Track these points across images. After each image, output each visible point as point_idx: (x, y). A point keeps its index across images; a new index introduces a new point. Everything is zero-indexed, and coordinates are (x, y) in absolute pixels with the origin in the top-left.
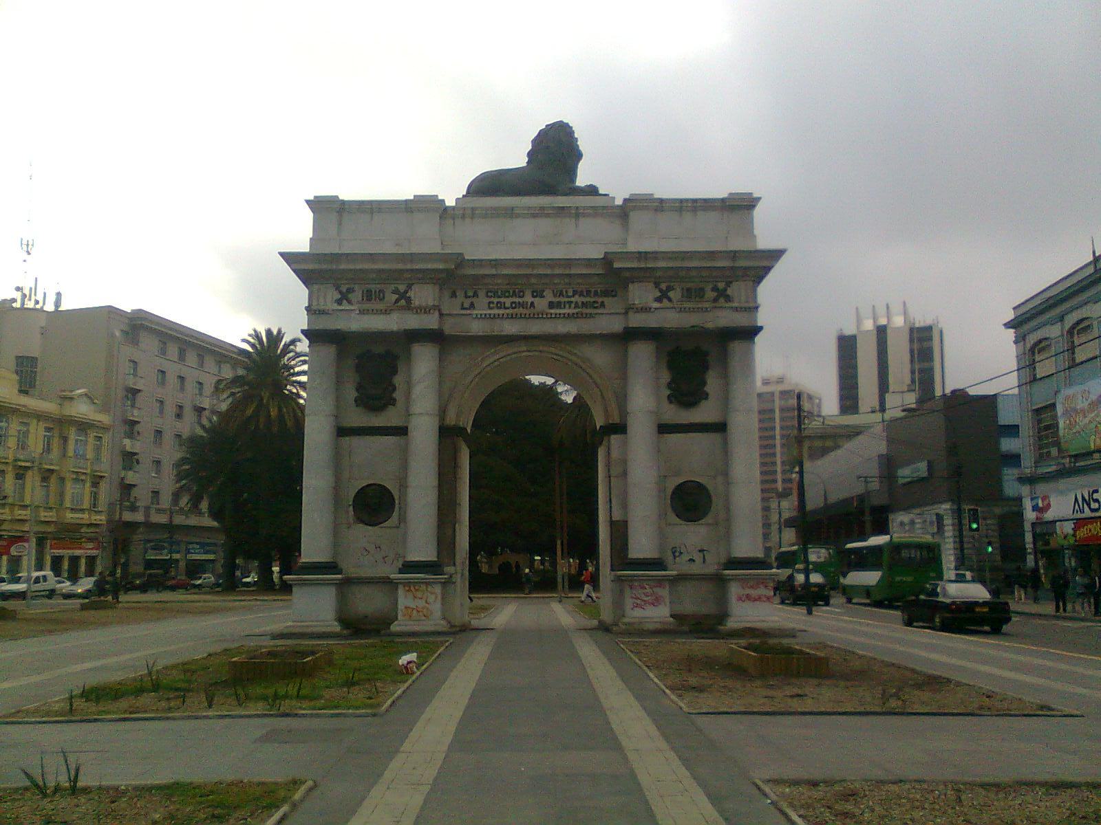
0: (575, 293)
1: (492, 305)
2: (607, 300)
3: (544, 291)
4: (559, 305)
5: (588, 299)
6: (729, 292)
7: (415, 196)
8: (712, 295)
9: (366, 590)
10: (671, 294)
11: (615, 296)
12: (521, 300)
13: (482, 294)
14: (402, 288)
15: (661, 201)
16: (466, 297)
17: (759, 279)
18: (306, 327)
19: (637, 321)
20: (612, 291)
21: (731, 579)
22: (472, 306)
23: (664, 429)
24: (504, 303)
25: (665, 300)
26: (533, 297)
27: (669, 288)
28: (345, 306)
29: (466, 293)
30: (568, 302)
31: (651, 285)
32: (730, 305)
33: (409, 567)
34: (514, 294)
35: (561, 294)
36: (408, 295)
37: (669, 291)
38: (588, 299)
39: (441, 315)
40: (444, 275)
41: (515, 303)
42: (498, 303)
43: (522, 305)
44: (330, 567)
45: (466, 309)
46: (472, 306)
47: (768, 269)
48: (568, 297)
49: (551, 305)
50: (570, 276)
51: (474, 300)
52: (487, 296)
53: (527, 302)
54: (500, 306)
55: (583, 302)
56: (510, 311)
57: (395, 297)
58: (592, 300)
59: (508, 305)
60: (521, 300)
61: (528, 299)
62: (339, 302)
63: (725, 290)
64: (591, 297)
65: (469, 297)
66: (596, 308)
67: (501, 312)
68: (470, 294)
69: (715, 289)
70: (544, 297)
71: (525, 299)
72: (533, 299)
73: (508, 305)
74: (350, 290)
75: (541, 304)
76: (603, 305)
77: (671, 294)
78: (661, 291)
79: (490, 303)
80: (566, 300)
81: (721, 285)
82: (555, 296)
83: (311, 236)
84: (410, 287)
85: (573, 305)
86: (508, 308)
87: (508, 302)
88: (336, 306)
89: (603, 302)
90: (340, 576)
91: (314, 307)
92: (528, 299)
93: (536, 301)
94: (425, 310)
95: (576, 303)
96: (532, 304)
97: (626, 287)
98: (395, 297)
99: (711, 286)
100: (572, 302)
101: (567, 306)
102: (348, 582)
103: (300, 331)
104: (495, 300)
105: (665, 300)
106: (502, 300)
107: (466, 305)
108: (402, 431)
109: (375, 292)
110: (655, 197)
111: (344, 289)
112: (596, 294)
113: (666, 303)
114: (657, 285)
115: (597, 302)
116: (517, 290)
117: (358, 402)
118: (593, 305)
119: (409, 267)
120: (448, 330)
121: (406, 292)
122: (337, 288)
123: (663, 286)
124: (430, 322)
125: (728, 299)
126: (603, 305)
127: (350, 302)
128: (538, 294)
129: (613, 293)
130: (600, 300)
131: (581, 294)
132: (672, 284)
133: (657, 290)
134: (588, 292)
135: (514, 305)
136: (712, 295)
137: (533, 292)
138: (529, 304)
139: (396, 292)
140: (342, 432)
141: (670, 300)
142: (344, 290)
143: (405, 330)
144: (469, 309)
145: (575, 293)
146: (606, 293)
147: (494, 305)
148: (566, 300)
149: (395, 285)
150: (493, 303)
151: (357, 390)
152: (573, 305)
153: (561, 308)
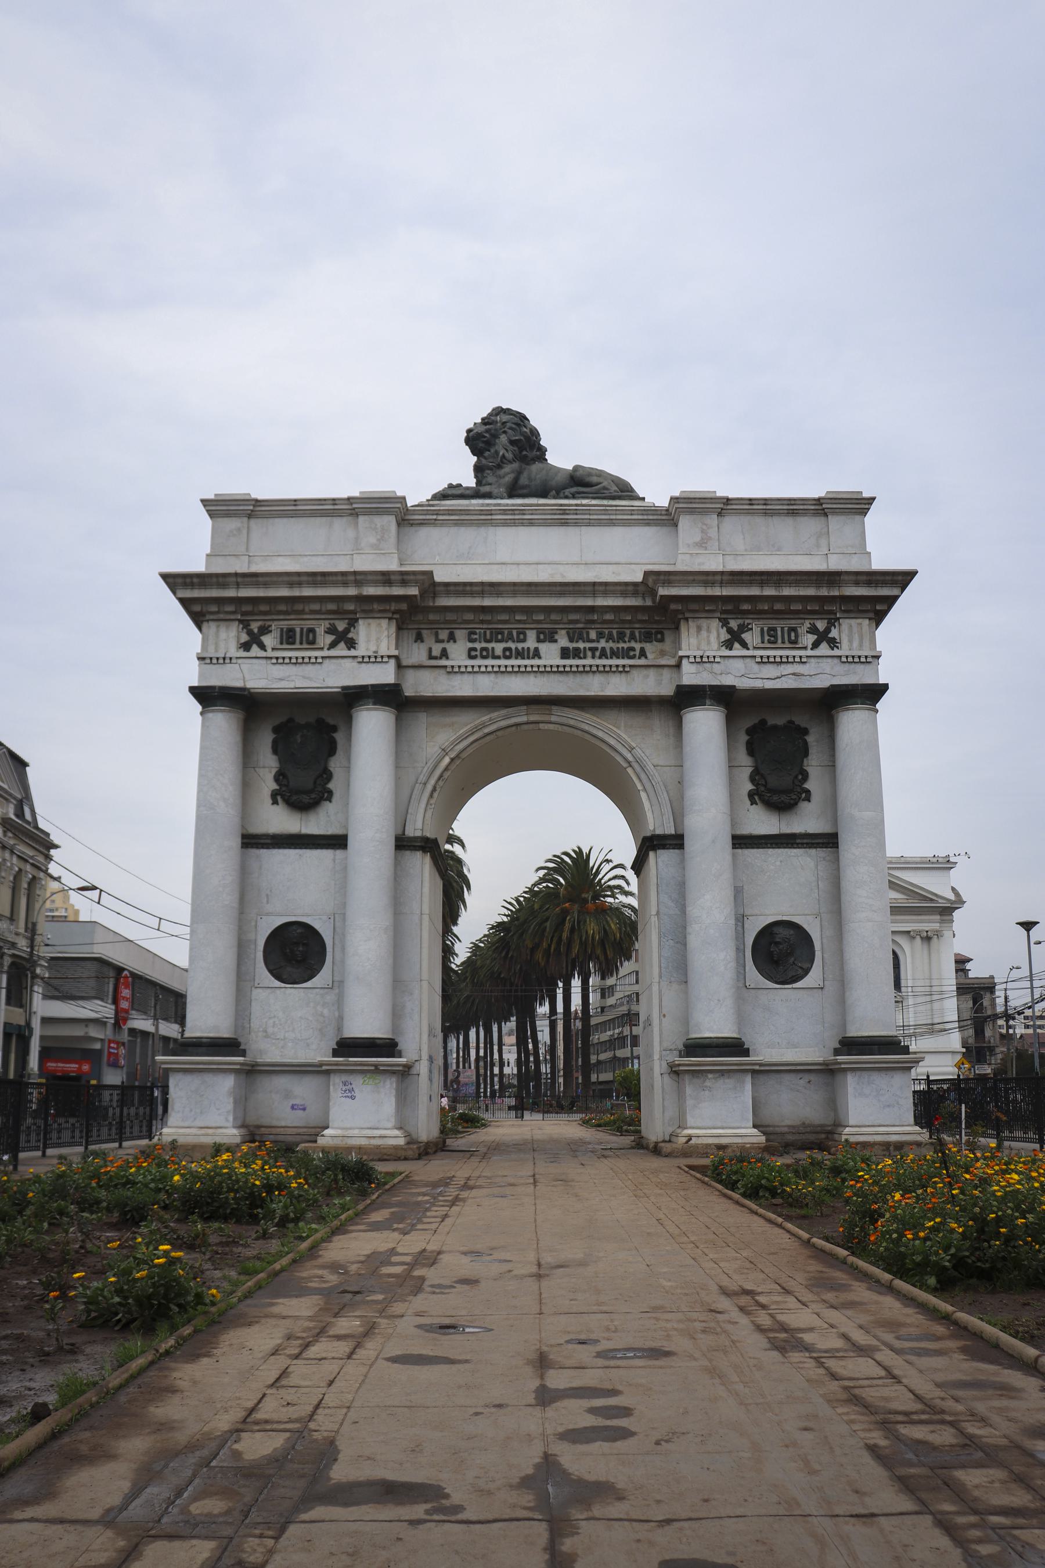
0: (600, 635)
1: (473, 653)
2: (649, 647)
3: (556, 633)
4: (577, 654)
5: (621, 645)
6: (834, 633)
7: (361, 493)
8: (811, 638)
9: (281, 1082)
10: (746, 636)
11: (662, 640)
12: (520, 646)
13: (460, 634)
14: (341, 626)
15: (728, 501)
16: (438, 641)
17: (878, 617)
18: (195, 683)
19: (691, 676)
20: (657, 633)
21: (845, 1070)
22: (444, 654)
23: (740, 842)
24: (493, 648)
25: (736, 645)
26: (539, 641)
27: (743, 628)
28: (255, 650)
29: (437, 634)
30: (590, 649)
31: (715, 624)
32: (836, 652)
33: (347, 1047)
34: (510, 638)
35: (581, 638)
36: (350, 635)
37: (743, 632)
38: (621, 645)
39: (400, 667)
40: (404, 606)
41: (510, 649)
42: (483, 649)
43: (520, 654)
44: (229, 1046)
45: (435, 658)
46: (444, 654)
47: (892, 600)
48: (593, 641)
49: (565, 653)
50: (592, 609)
51: (451, 647)
52: (471, 641)
53: (528, 648)
54: (486, 653)
55: (611, 648)
56: (503, 662)
57: (330, 638)
58: (625, 646)
59: (499, 651)
60: (520, 646)
61: (531, 643)
62: (246, 646)
63: (828, 630)
64: (625, 642)
65: (442, 641)
66: (633, 657)
67: (490, 662)
68: (444, 635)
69: (813, 630)
70: (556, 641)
71: (525, 645)
72: (536, 645)
73: (499, 651)
74: (265, 630)
75: (550, 654)
76: (643, 654)
77: (743, 636)
78: (730, 631)
79: (471, 650)
80: (588, 645)
81: (821, 625)
82: (571, 640)
83: (208, 551)
84: (353, 623)
85: (598, 654)
86: (498, 657)
87: (499, 648)
88: (242, 653)
89: (642, 650)
90: (241, 1059)
91: (211, 653)
92: (531, 643)
93: (543, 648)
94: (375, 659)
95: (603, 649)
96: (536, 650)
97: (677, 628)
98: (330, 638)
99: (807, 624)
100: (596, 649)
101: (589, 654)
102: (252, 1072)
103: (187, 689)
104: (478, 645)
105: (736, 645)
106: (490, 646)
107: (437, 650)
108: (338, 842)
109: (302, 629)
110: (719, 494)
111: (255, 626)
112: (632, 637)
113: (738, 650)
114: (725, 623)
115: (633, 649)
116: (515, 633)
117: (274, 797)
118: (627, 654)
119: (352, 591)
120: (409, 692)
121: (347, 631)
122: (245, 624)
123: (734, 624)
124: (384, 675)
125: (833, 643)
126: (643, 654)
127: (263, 647)
128: (550, 637)
129: (659, 636)
130: (637, 646)
131: (610, 638)
132: (747, 621)
133: (725, 629)
134: (621, 637)
135: (507, 654)
136: (811, 638)
137: (540, 632)
138: (532, 650)
139: (332, 630)
140: (251, 841)
141: (744, 645)
142: (256, 631)
143: (344, 688)
144: (441, 658)
145: (600, 635)
146: (648, 637)
147: (478, 653)
148: (588, 645)
149: (332, 622)
150: (475, 649)
151: (276, 779)
152: (598, 654)
153: (581, 658)
